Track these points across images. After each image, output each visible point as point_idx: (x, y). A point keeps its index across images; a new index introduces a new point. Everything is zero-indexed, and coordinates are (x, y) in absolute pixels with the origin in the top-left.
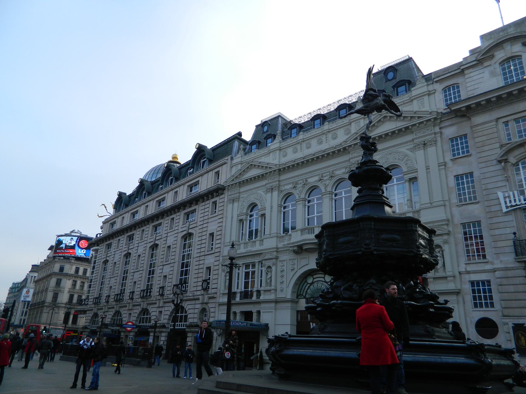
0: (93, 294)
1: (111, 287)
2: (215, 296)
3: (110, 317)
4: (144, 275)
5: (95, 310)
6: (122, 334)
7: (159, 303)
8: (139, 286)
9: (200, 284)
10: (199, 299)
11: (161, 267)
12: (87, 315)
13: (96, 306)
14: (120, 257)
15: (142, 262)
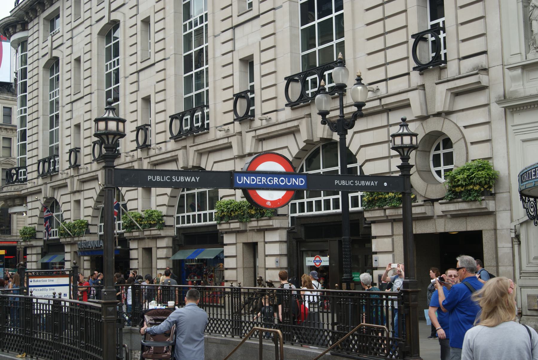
0: (35, 153)
1: (78, 126)
2: (484, 79)
3: (91, 203)
4: (171, 71)
5: (47, 192)
6: (133, 245)
7: (242, 144)
8: (160, 107)
9: (403, 51)
10: (408, 106)
11: (228, 35)
12: (30, 206)
13: (48, 180)
14: (88, 39)
15: (160, 36)
